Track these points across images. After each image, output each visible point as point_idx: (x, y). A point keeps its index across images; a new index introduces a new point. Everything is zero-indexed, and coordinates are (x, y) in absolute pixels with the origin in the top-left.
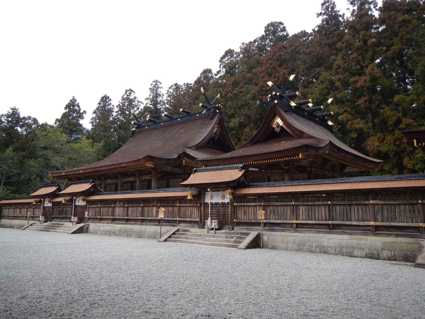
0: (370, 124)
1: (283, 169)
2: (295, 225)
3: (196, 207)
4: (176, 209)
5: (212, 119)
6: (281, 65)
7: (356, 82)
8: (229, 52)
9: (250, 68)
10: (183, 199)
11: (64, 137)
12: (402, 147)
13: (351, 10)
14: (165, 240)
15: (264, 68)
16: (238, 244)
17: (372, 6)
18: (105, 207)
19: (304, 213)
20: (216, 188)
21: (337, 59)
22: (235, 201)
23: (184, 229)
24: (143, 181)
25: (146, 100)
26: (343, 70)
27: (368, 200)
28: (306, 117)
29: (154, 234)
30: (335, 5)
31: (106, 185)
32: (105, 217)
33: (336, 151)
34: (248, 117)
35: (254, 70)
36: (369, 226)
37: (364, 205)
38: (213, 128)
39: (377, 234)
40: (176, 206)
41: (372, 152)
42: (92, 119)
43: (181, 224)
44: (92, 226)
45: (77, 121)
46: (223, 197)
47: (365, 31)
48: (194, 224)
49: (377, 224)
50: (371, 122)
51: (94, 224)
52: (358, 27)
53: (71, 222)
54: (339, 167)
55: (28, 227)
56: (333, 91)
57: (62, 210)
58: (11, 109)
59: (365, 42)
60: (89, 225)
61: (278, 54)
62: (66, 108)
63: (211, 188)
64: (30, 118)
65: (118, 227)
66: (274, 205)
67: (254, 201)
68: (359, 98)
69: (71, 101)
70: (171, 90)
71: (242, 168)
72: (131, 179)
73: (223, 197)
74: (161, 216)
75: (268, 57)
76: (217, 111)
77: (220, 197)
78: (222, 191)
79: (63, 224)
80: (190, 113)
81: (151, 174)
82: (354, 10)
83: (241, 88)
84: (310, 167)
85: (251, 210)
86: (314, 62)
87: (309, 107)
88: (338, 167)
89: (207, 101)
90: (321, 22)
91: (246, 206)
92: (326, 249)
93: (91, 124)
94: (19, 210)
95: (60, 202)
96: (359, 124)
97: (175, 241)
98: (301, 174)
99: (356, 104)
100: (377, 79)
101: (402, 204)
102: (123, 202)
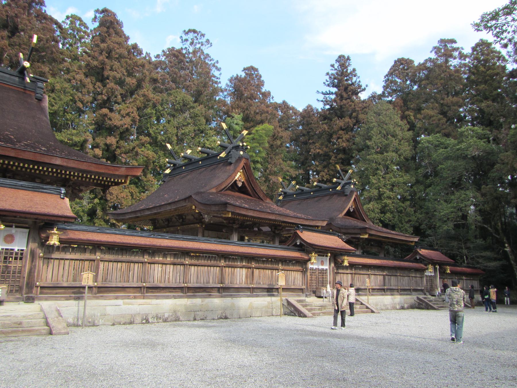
20: (320, 252)
29: (249, 311)
36: (398, 289)
48: (298, 292)
65: (167, 304)
85: (345, 276)
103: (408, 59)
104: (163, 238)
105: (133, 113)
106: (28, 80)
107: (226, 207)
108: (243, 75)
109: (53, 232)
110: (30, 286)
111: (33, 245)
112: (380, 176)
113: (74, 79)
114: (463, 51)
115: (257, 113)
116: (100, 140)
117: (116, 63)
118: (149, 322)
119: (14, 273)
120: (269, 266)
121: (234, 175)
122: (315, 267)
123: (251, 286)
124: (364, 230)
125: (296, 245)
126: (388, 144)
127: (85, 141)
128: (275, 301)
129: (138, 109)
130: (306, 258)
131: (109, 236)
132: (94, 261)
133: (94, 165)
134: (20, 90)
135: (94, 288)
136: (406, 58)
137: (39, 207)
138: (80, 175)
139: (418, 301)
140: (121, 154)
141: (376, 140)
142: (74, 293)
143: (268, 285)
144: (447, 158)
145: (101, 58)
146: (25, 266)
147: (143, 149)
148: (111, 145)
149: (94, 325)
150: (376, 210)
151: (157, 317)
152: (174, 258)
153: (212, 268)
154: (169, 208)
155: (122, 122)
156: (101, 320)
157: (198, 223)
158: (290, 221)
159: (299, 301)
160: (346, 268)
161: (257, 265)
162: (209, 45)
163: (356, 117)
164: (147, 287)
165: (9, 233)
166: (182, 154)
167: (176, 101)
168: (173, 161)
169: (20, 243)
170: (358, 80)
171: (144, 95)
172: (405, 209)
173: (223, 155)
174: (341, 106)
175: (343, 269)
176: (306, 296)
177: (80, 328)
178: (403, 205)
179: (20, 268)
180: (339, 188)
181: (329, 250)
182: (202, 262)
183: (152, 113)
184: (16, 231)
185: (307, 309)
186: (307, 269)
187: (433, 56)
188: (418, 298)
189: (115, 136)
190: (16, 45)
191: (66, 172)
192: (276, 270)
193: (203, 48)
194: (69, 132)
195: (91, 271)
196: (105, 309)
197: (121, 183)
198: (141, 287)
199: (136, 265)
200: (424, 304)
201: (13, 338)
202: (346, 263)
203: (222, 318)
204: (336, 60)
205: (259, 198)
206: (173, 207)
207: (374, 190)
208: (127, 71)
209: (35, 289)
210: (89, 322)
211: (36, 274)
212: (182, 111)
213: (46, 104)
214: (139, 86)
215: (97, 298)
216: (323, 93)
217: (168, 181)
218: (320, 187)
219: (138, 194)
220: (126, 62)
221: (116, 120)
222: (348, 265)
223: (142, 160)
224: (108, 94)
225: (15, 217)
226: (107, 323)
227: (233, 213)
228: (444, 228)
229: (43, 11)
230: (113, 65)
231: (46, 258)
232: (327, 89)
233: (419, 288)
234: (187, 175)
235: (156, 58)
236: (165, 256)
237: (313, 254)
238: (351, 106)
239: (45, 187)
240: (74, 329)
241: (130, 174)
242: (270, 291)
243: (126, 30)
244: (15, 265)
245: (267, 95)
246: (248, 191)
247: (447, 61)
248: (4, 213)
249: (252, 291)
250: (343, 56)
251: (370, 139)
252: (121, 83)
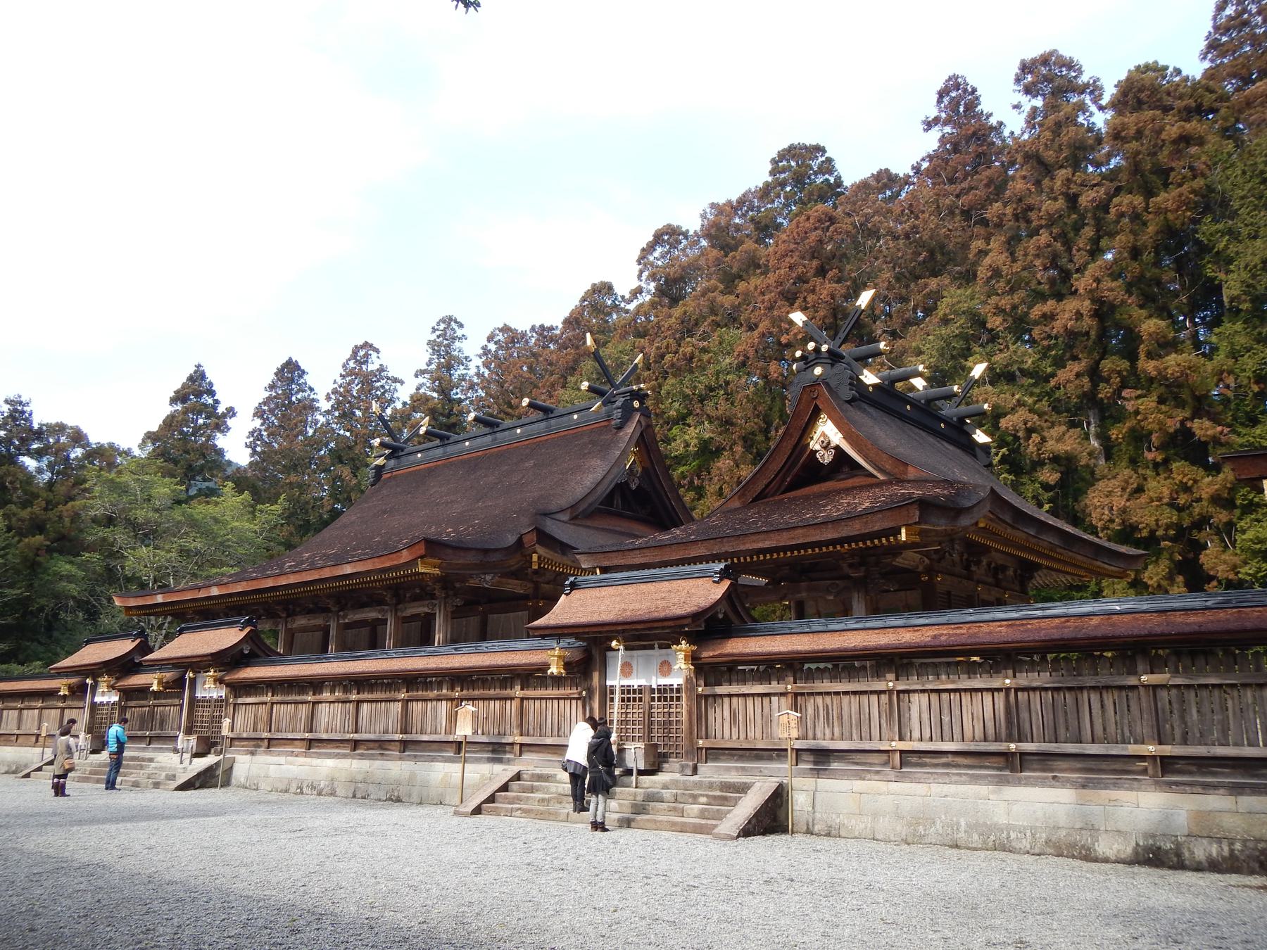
0: (1095, 443)
1: (848, 577)
2: (898, 755)
3: (577, 699)
4: (512, 707)
5: (620, 428)
6: (822, 272)
7: (1049, 318)
8: (668, 236)
9: (730, 281)
10: (531, 676)
11: (164, 489)
12: (1197, 510)
13: (1027, 108)
14: (477, 811)
15: (771, 278)
16: (714, 822)
17: (1087, 99)
19: (925, 716)
20: (639, 638)
21: (990, 250)
22: (702, 682)
23: (538, 771)
24: (406, 620)
25: (416, 376)
26: (1009, 282)
27: (1133, 672)
28: (911, 419)
30: (977, 98)
31: (291, 635)
32: (284, 735)
33: (1008, 518)
34: (727, 423)
35: (742, 286)
36: (1142, 758)
37: (1121, 688)
38: (624, 453)
39: (1170, 784)
40: (512, 699)
41: (1105, 528)
42: (252, 433)
43: (526, 756)
44: (245, 765)
45: (209, 438)
46: (665, 668)
47: (1070, 170)
49: (1167, 750)
50: (1098, 436)
51: (248, 757)
52: (1049, 156)
53: (176, 751)
54: (1015, 572)
55: (39, 769)
56: (981, 345)
57: (152, 714)
58: (6, 402)
59: (1072, 200)
60: (234, 760)
61: (813, 236)
62: (173, 401)
63: (625, 640)
64: (60, 428)
65: (327, 766)
66: (828, 693)
67: (764, 677)
68: (1059, 363)
69: (191, 378)
70: (492, 347)
71: (724, 574)
72: (371, 614)
73: (665, 668)
74: (464, 729)
75: (782, 247)
76: (636, 404)
77: (655, 666)
78: (661, 647)
79: (151, 760)
80: (552, 411)
81: (433, 597)
82: (1034, 109)
83: (704, 339)
84: (930, 571)
86: (921, 259)
87: (913, 388)
88: (1010, 572)
89: (605, 373)
90: (935, 145)
91: (738, 696)
92: (1004, 835)
93: (249, 451)
94: (16, 712)
95: (143, 691)
96: (1061, 440)
97: (509, 813)
98: (902, 594)
99: (1053, 383)
100: (1113, 307)
101: (1245, 686)
102: (345, 687)
158: (761, 545)
215: (270, 753)
242: (497, 750)
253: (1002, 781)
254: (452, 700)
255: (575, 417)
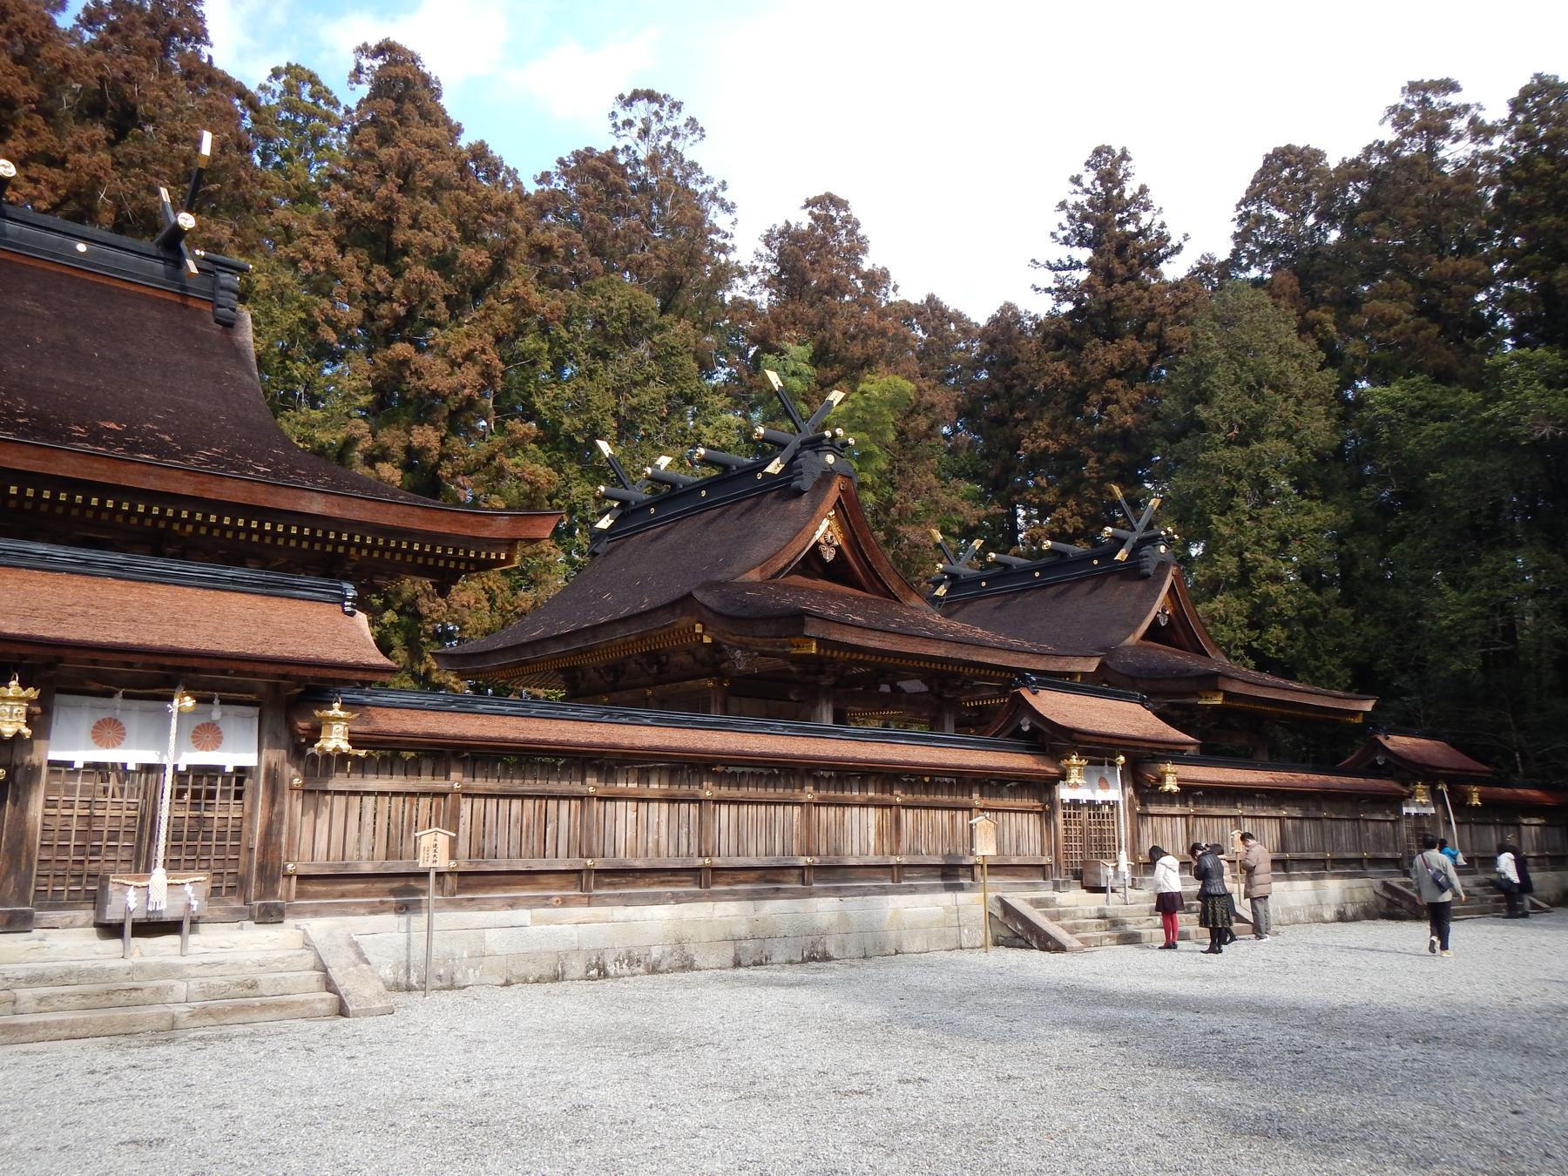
18: (511, 797)
32: (520, 866)
36: (1324, 860)
48: (1030, 877)
65: (654, 920)
85: (1166, 822)
103: (1307, 148)
104: (635, 722)
105: (483, 351)
106: (192, 267)
107: (803, 624)
108: (803, 220)
109: (331, 713)
110: (270, 873)
111: (276, 756)
112: (1244, 512)
113: (307, 257)
114: (1482, 115)
115: (853, 338)
116: (392, 438)
117: (427, 203)
118: (606, 976)
119: (222, 836)
120: (945, 798)
121: (810, 527)
122: (1084, 795)
123: (893, 860)
124: (1210, 681)
125: (1017, 733)
126: (1264, 413)
127: (350, 443)
128: (970, 905)
129: (499, 339)
130: (1052, 770)
131: (483, 720)
132: (445, 795)
133: (419, 512)
134: (169, 297)
135: (448, 878)
136: (1300, 144)
137: (290, 641)
138: (381, 542)
139: (1388, 896)
140: (454, 475)
141: (1226, 402)
142: (392, 892)
143: (944, 857)
144: (1454, 449)
145: (383, 192)
146: (252, 816)
147: (516, 459)
148: (424, 450)
149: (452, 987)
150: (1235, 617)
151: (630, 958)
152: (670, 784)
153: (780, 809)
154: (621, 632)
155: (453, 381)
156: (471, 971)
157: (709, 676)
158: (989, 661)
159: (1038, 903)
160: (1170, 798)
161: (909, 796)
162: (696, 136)
163: (1159, 335)
164: (597, 871)
165: (205, 721)
166: (649, 470)
167: (610, 310)
168: (620, 492)
169: (238, 751)
170: (1157, 222)
171: (515, 298)
172: (1325, 612)
173: (774, 467)
174: (1109, 303)
175: (1159, 803)
176: (1056, 887)
177: (418, 995)
178: (1318, 599)
179: (238, 822)
180: (1122, 555)
181: (1119, 746)
182: (751, 792)
183: (541, 349)
184: (224, 715)
185: (1063, 927)
186: (1052, 802)
187: (1389, 134)
188: (1386, 886)
189: (433, 424)
190: (132, 164)
191: (338, 535)
192: (963, 809)
193: (678, 145)
194: (301, 418)
195: (437, 825)
196: (482, 938)
197: (498, 563)
198: (579, 872)
199: (564, 805)
200: (1405, 904)
201: (240, 1029)
202: (1171, 785)
203: (814, 959)
204: (1087, 163)
205: (888, 594)
206: (636, 629)
207: (1227, 557)
208: (461, 226)
209: (283, 882)
210: (439, 977)
211: (284, 839)
212: (630, 341)
213: (247, 334)
214: (498, 271)
215: (458, 905)
216: (1050, 267)
217: (608, 553)
218: (1063, 554)
219: (508, 593)
220: (458, 202)
221: (436, 375)
222: (1176, 789)
223: (514, 492)
224: (407, 298)
225: (225, 672)
226: (489, 979)
227: (822, 642)
228: (1453, 667)
229: (205, 60)
230: (418, 213)
231: (311, 792)
232: (1062, 253)
233: (1388, 855)
234: (666, 531)
235: (538, 182)
236: (644, 777)
237: (1074, 760)
238: (1139, 300)
239: (297, 581)
240: (402, 997)
241: (524, 535)
242: (951, 873)
243: (452, 104)
244: (223, 812)
245: (876, 280)
246: (854, 572)
247: (1431, 150)
248: (195, 663)
249: (893, 875)
250: (1109, 150)
251: (1205, 398)
252: (443, 264)
253: (1289, 878)
254: (883, 806)
255: (82, 247)
